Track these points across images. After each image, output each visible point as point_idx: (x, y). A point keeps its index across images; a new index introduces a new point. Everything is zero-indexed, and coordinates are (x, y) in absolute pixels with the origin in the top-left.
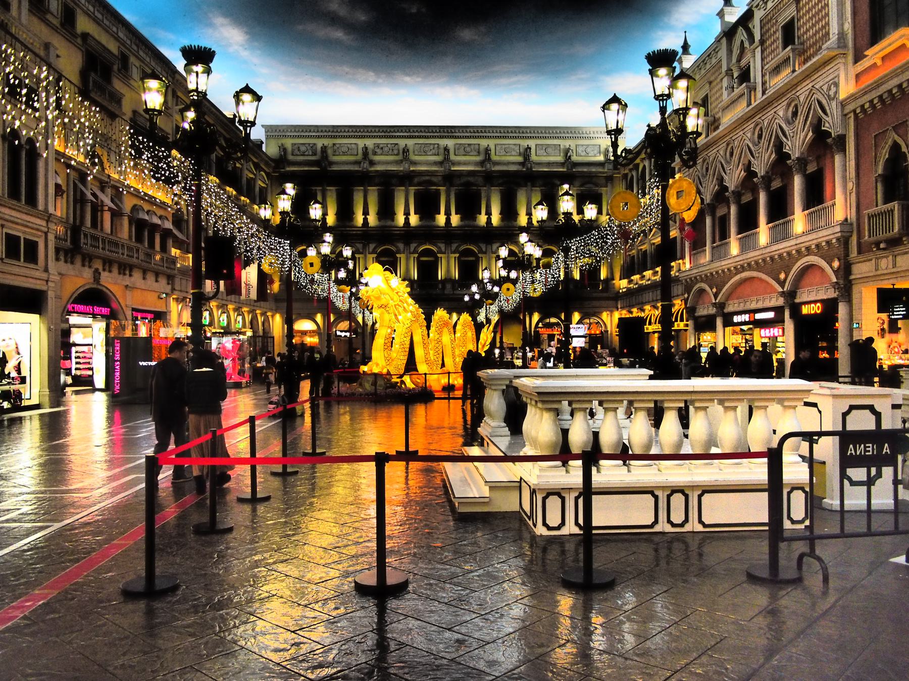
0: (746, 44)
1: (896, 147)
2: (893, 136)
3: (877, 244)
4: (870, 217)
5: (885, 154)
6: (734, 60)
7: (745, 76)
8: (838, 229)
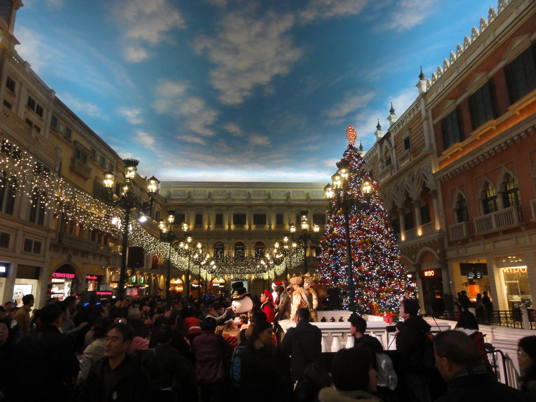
0: (388, 147)
1: (460, 196)
2: (458, 191)
3: (457, 242)
4: (453, 229)
5: (456, 199)
6: (383, 154)
7: (389, 161)
8: (437, 234)
